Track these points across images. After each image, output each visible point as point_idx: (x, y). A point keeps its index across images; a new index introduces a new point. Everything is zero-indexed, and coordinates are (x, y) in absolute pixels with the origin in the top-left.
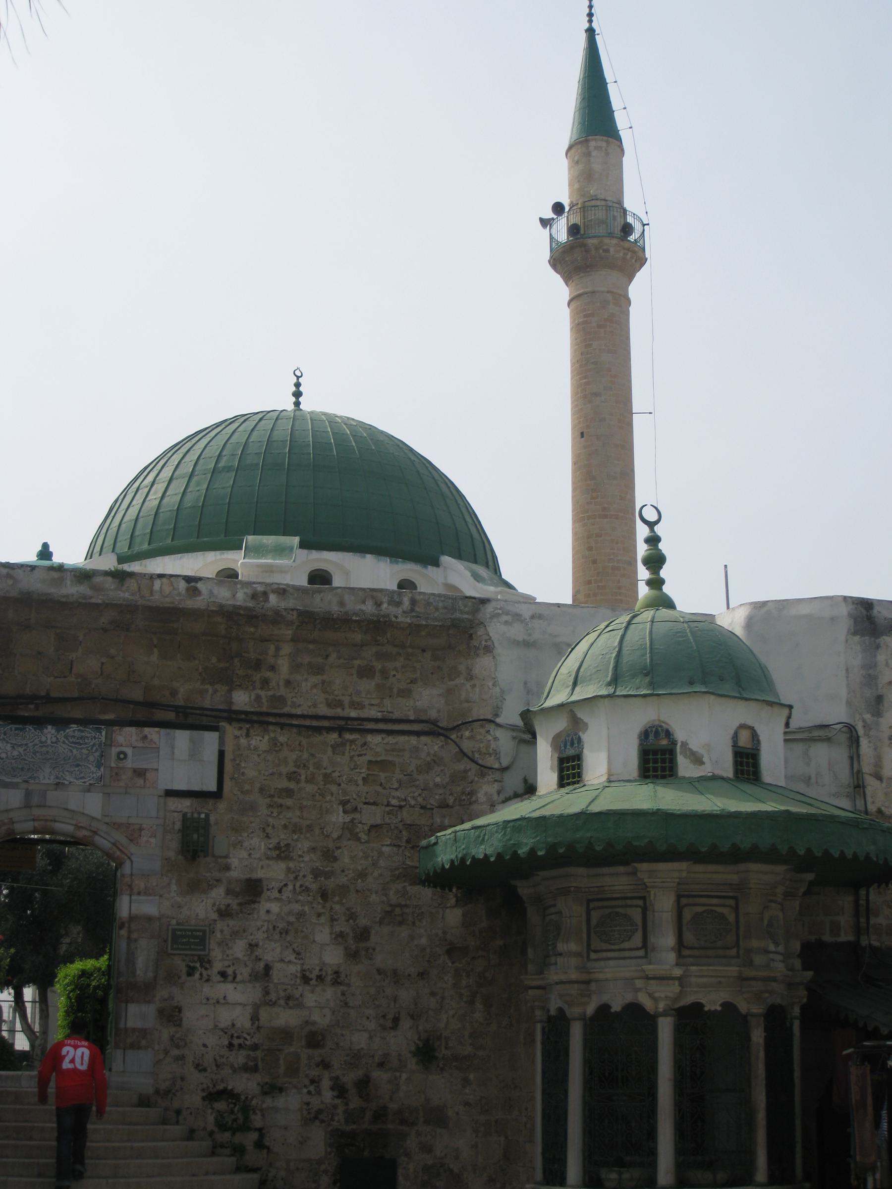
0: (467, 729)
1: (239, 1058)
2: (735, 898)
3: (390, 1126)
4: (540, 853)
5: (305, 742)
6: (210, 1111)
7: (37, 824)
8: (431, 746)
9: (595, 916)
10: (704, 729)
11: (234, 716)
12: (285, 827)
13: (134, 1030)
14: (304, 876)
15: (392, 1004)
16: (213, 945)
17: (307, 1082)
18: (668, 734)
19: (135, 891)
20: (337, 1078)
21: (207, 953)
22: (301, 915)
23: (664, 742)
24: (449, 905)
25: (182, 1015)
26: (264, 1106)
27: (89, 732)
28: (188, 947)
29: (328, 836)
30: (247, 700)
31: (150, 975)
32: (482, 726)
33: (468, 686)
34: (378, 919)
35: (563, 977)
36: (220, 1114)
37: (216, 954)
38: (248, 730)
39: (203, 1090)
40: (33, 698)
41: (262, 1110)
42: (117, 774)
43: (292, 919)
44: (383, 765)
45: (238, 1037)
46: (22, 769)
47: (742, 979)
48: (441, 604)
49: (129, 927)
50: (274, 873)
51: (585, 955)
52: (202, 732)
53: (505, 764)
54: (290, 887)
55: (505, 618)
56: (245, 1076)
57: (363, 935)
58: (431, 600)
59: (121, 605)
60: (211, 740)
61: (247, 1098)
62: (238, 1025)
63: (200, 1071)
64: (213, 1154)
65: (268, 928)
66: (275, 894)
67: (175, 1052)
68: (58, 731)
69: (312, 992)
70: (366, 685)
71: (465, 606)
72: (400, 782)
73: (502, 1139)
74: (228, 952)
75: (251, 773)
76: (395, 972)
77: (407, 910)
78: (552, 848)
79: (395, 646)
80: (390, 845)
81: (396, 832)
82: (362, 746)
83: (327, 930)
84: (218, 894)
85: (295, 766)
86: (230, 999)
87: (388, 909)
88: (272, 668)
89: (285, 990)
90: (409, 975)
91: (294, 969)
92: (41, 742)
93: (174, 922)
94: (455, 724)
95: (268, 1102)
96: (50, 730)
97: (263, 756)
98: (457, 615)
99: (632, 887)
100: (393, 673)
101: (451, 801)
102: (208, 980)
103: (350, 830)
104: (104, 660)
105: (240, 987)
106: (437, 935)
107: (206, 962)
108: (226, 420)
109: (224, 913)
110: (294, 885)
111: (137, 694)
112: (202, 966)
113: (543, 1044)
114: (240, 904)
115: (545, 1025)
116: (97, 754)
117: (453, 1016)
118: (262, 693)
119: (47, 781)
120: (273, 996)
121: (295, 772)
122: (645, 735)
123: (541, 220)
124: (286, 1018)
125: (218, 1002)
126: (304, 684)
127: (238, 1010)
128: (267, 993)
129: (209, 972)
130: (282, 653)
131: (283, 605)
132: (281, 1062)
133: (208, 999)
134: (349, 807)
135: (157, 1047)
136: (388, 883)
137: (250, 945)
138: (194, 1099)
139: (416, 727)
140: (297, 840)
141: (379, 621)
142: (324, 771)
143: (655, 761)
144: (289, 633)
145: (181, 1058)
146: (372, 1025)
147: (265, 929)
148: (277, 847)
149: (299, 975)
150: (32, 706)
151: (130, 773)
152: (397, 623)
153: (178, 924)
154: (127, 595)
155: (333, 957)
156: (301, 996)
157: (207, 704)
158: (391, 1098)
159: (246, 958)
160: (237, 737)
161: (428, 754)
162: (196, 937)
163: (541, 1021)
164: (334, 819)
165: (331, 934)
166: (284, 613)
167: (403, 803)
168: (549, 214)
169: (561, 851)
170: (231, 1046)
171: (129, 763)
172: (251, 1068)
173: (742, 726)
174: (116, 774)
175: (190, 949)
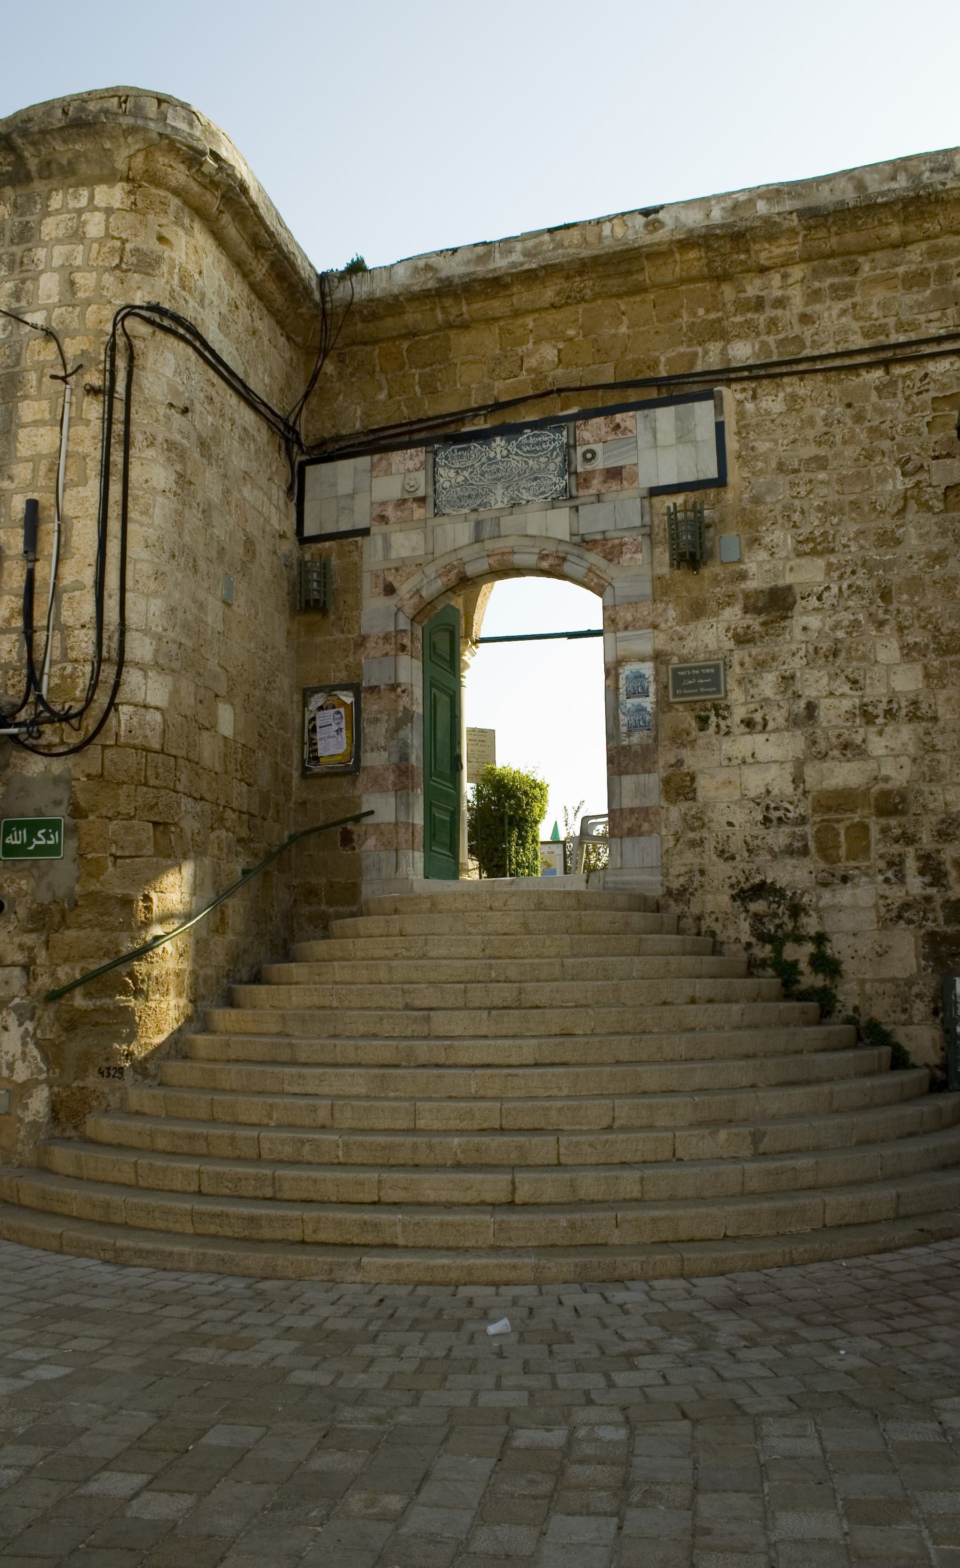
1: (779, 838)
5: (836, 390)
6: (743, 915)
13: (632, 811)
14: (853, 572)
16: (732, 684)
17: (882, 864)
19: (621, 626)
21: (722, 695)
25: (695, 785)
26: (821, 904)
27: (547, 436)
29: (883, 512)
36: (758, 918)
37: (736, 695)
38: (754, 391)
39: (732, 886)
41: (817, 910)
42: (585, 480)
43: (840, 634)
45: (776, 809)
46: (469, 497)
50: (809, 574)
52: (690, 404)
56: (791, 862)
60: (704, 411)
61: (794, 893)
62: (775, 792)
63: (726, 860)
64: (750, 974)
65: (807, 651)
66: (814, 602)
68: (508, 442)
69: (880, 733)
74: (752, 691)
83: (895, 645)
85: (826, 425)
86: (761, 756)
89: (840, 735)
92: (489, 459)
95: (827, 897)
97: (778, 422)
102: (728, 733)
105: (773, 737)
107: (721, 710)
110: (840, 589)
112: (717, 715)
114: (763, 624)
118: (771, 339)
119: (500, 505)
120: (823, 746)
121: (826, 434)
124: (844, 775)
125: (744, 762)
126: (826, 314)
127: (774, 770)
128: (814, 743)
129: (728, 722)
132: (842, 838)
133: (730, 760)
134: (910, 467)
135: (664, 832)
137: (783, 678)
140: (838, 524)
141: (918, 197)
142: (869, 424)
147: (802, 653)
149: (857, 712)
155: (907, 681)
156: (864, 741)
157: (699, 368)
159: (778, 697)
160: (740, 403)
165: (902, 648)
166: (777, 219)
170: (766, 821)
175: (699, 694)
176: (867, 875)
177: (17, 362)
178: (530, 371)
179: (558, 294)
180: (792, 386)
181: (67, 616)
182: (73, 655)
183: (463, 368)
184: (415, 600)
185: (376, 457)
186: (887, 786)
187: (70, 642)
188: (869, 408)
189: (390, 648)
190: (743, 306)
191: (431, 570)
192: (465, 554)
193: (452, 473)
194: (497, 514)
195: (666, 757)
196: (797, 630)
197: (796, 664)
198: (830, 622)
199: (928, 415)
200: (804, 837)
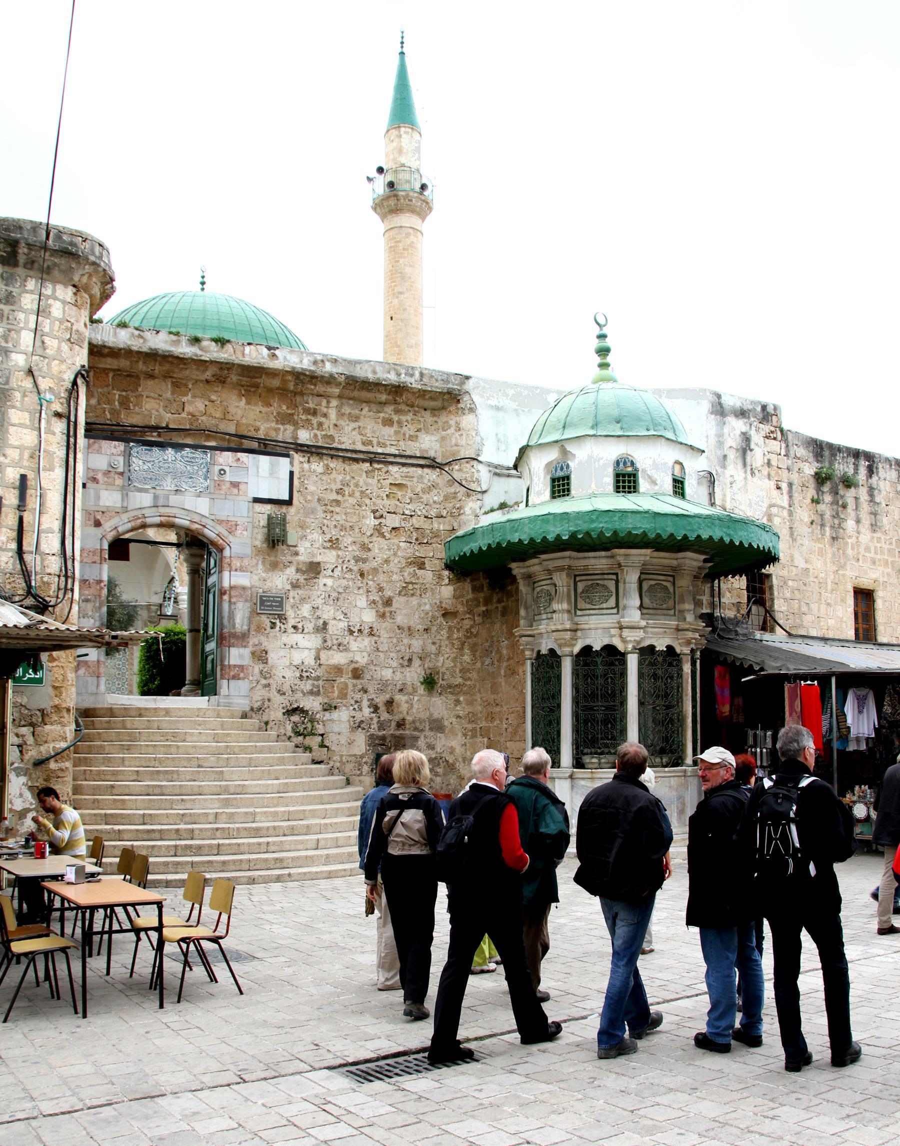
1: (307, 686)
2: (673, 576)
3: (407, 732)
4: (564, 538)
5: (347, 468)
7: (162, 519)
8: (431, 475)
9: (581, 586)
10: (654, 461)
11: (301, 448)
12: (335, 526)
17: (353, 703)
18: (632, 463)
19: (234, 568)
20: (373, 699)
22: (346, 588)
23: (630, 469)
27: (198, 454)
28: (271, 607)
30: (308, 437)
31: (245, 627)
33: (457, 434)
35: (560, 627)
37: (290, 613)
39: (283, 708)
40: (155, 428)
41: (323, 722)
43: (341, 590)
44: (399, 486)
46: (151, 479)
47: (678, 630)
48: (439, 378)
49: (230, 594)
50: (328, 558)
53: (484, 489)
54: (339, 568)
56: (312, 698)
57: (388, 602)
59: (222, 363)
62: (306, 663)
66: (329, 572)
67: (264, 682)
70: (389, 431)
72: (411, 499)
73: (486, 740)
75: (312, 488)
77: (416, 586)
78: (573, 535)
79: (407, 405)
83: (364, 598)
84: (291, 571)
86: (300, 645)
88: (325, 415)
91: (343, 625)
93: (261, 591)
96: (170, 451)
98: (450, 386)
101: (444, 513)
103: (378, 531)
104: (207, 403)
105: (307, 636)
107: (282, 618)
108: (140, 303)
109: (295, 586)
111: (232, 429)
112: (280, 622)
113: (532, 674)
116: (205, 470)
118: (318, 433)
120: (329, 643)
123: (368, 178)
124: (337, 658)
128: (325, 641)
129: (286, 626)
130: (331, 405)
131: (334, 370)
134: (377, 514)
135: (251, 678)
138: (276, 714)
139: (422, 462)
143: (624, 482)
144: (337, 391)
145: (268, 685)
146: (395, 664)
147: (323, 597)
148: (330, 541)
150: (155, 434)
151: (228, 485)
152: (411, 388)
153: (264, 592)
154: (226, 356)
155: (369, 617)
157: (280, 438)
158: (408, 713)
161: (429, 480)
162: (276, 602)
164: (368, 522)
168: (374, 174)
169: (580, 536)
171: (228, 478)
172: (314, 693)
173: (677, 462)
174: (218, 486)
175: (272, 610)
176: (345, 706)
177: (7, 383)
178: (189, 414)
179: (213, 376)
180: (327, 461)
181: (44, 547)
182: (48, 571)
183: (148, 399)
184: (114, 533)
185: (92, 441)
186: (357, 666)
187: (46, 563)
188: (361, 480)
189: (97, 558)
190: (308, 411)
191: (125, 517)
192: (147, 512)
193: (141, 462)
194: (167, 493)
195: (253, 640)
196: (321, 585)
197: (320, 602)
198: (337, 583)
200: (318, 686)
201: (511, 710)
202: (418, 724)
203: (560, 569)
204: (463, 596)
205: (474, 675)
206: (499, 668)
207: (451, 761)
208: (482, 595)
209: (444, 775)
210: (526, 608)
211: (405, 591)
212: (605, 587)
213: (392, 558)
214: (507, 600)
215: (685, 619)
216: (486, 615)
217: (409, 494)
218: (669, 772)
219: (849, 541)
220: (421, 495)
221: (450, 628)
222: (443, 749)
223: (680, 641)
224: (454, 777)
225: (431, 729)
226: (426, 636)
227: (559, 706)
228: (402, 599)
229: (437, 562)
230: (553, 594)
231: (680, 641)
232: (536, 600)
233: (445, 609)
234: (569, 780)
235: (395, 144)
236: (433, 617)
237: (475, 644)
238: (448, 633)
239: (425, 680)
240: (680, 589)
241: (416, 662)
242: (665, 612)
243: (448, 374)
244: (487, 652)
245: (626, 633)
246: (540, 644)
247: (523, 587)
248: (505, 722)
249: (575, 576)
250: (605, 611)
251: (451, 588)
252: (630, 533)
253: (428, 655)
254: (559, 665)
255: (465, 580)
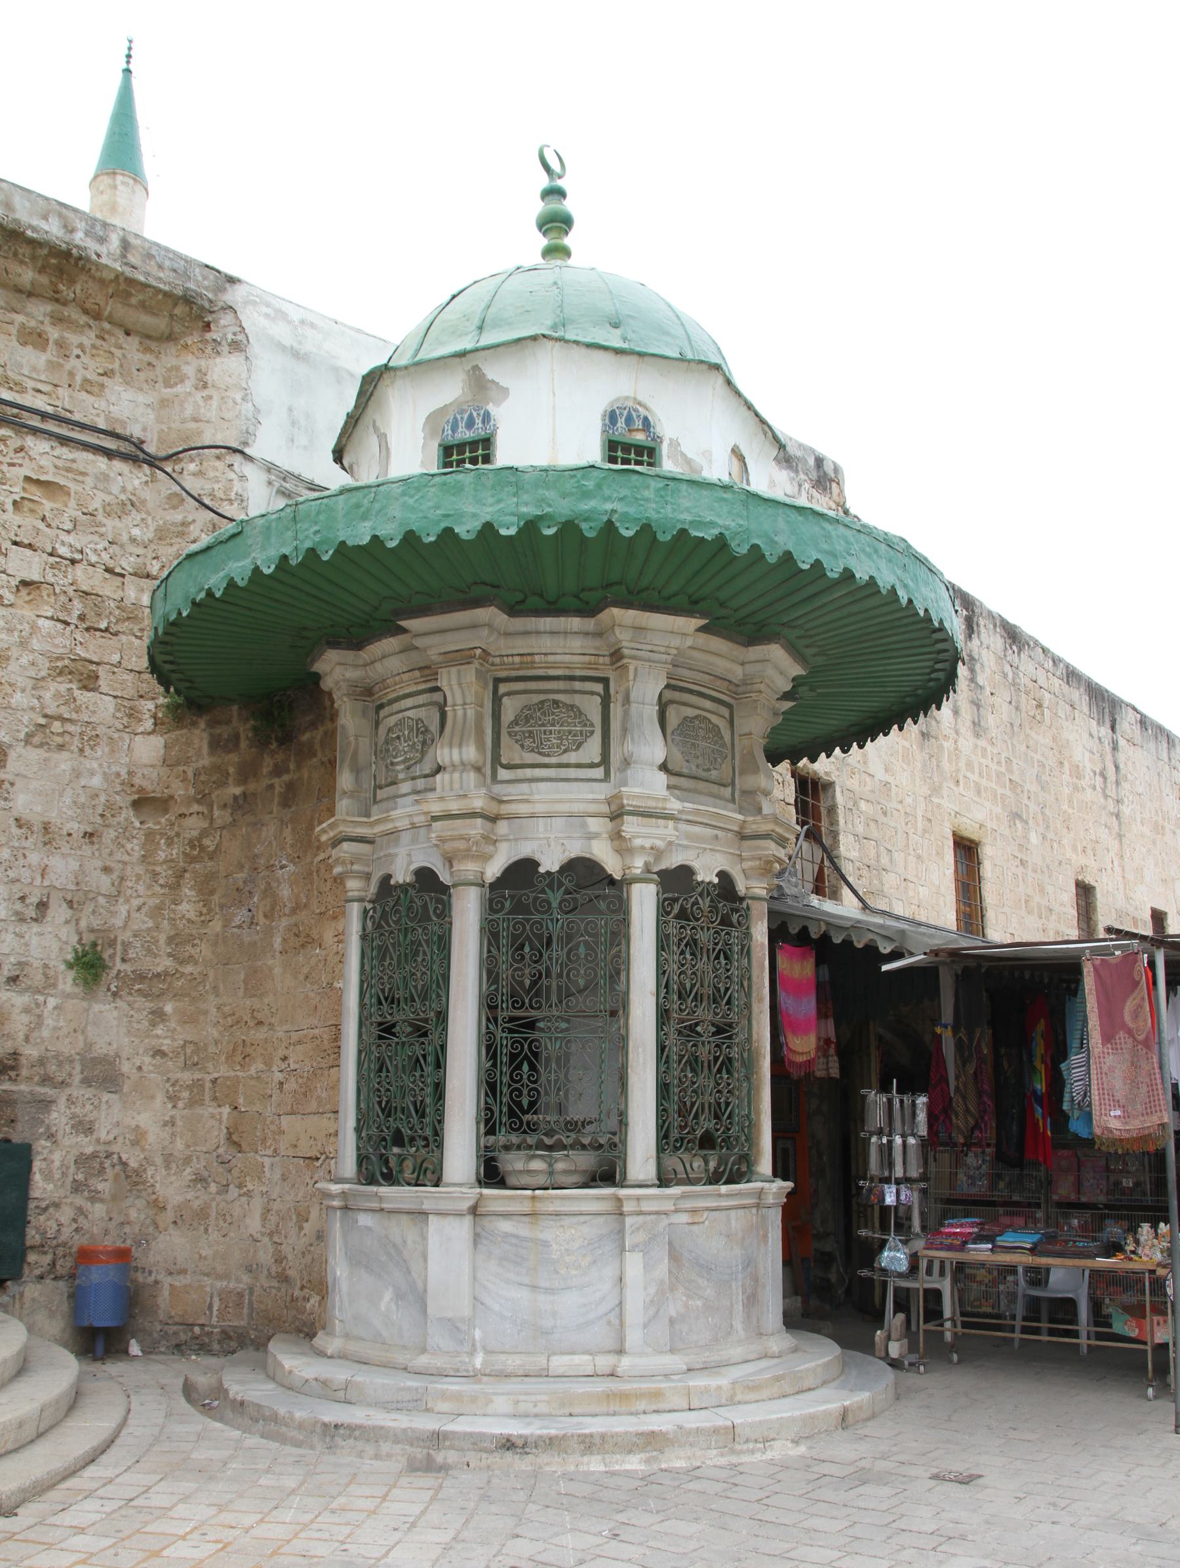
0: (192, 460)
3: (23, 1087)
8: (129, 479)
15: (38, 882)
18: (647, 425)
23: (640, 437)
24: (141, 729)
32: (218, 458)
33: (199, 395)
34: (22, 736)
35: (454, 806)
48: (167, 263)
51: (489, 772)
55: (264, 310)
58: (153, 252)
71: (205, 278)
72: (75, 522)
73: (226, 1110)
76: (46, 828)
77: (71, 728)
79: (86, 312)
80: (52, 618)
81: (63, 598)
82: (16, 451)
87: (42, 721)
90: (70, 835)
94: (171, 452)
98: (192, 286)
99: (587, 658)
100: (78, 352)
106: (118, 775)
113: (364, 937)
115: (369, 906)
117: (139, 909)
122: (612, 417)
136: (43, 678)
158: (27, 1039)
161: (124, 490)
163: (361, 900)
167: (78, 556)
199: (18, 492)
201: (295, 1036)
202: (52, 1068)
203: (461, 658)
204: (187, 761)
205: (203, 950)
206: (269, 932)
207: (133, 1164)
208: (234, 758)
209: (114, 1198)
210: (357, 770)
211: (40, 734)
212: (578, 713)
213: (14, 652)
214: (299, 767)
215: (759, 810)
216: (241, 805)
217: (72, 511)
218: (728, 1196)
219: (946, 744)
220: (100, 517)
221: (150, 836)
222: (115, 1132)
223: (747, 865)
224: (140, 1203)
225: (87, 1082)
226: (87, 850)
227: (442, 1017)
228: (34, 755)
229: (129, 677)
230: (434, 727)
231: (747, 865)
232: (383, 751)
233: (141, 790)
234: (468, 1220)
235: (105, 197)
236: (109, 806)
237: (211, 876)
238: (143, 846)
239: (77, 958)
240: (746, 742)
241: (59, 912)
242: (715, 789)
243: (188, 261)
244: (240, 895)
245: (631, 825)
246: (391, 857)
247: (349, 719)
248: (277, 1064)
249: (497, 681)
250: (572, 773)
251: (157, 742)
252: (683, 532)
253: (90, 896)
254: (445, 911)
255: (194, 724)
